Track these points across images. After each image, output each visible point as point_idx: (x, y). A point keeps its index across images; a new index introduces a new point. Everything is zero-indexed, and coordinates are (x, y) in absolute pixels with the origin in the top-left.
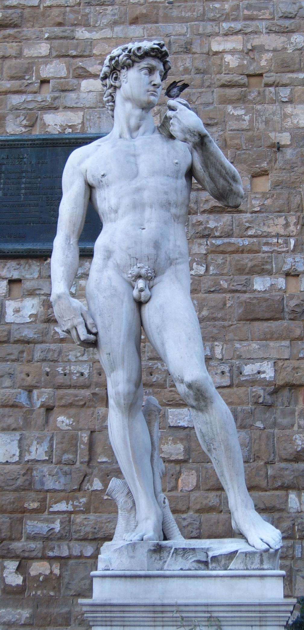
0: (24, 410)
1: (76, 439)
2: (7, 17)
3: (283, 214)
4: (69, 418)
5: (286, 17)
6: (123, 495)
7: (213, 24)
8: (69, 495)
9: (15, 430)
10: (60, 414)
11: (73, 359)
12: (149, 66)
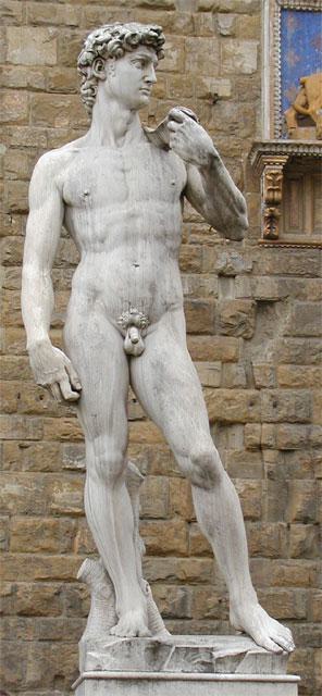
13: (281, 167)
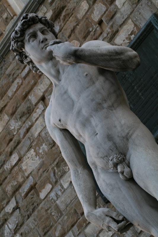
2: (55, 9)
12: (30, 35)
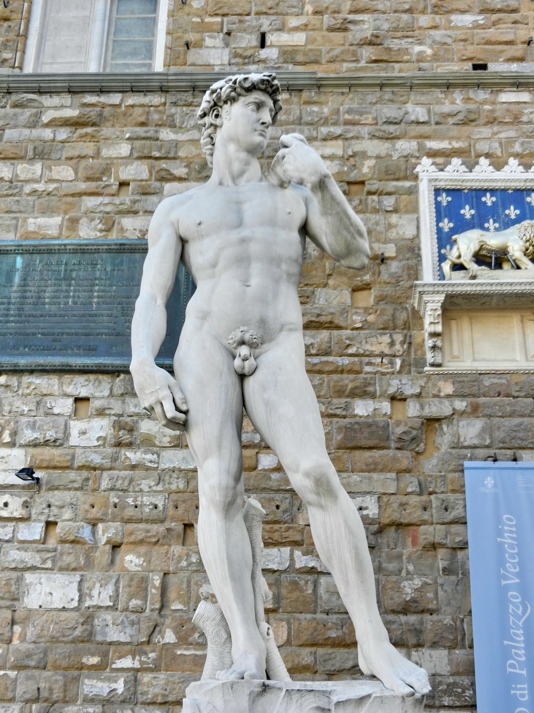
0: (87, 547)
1: (146, 582)
2: (85, 115)
3: (387, 331)
4: (139, 557)
5: (391, 123)
6: (214, 622)
7: (311, 127)
8: (136, 649)
9: (74, 569)
10: (127, 553)
11: (146, 489)
12: (256, 101)
13: (440, 304)
